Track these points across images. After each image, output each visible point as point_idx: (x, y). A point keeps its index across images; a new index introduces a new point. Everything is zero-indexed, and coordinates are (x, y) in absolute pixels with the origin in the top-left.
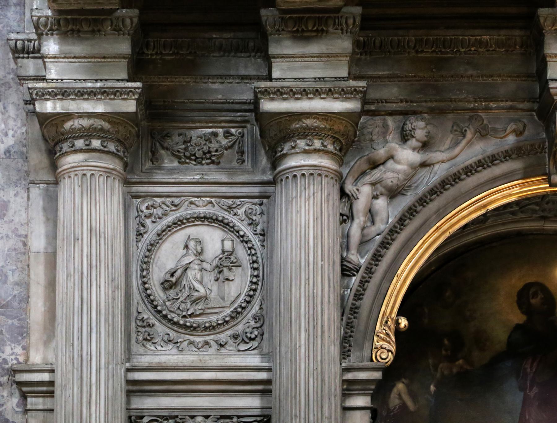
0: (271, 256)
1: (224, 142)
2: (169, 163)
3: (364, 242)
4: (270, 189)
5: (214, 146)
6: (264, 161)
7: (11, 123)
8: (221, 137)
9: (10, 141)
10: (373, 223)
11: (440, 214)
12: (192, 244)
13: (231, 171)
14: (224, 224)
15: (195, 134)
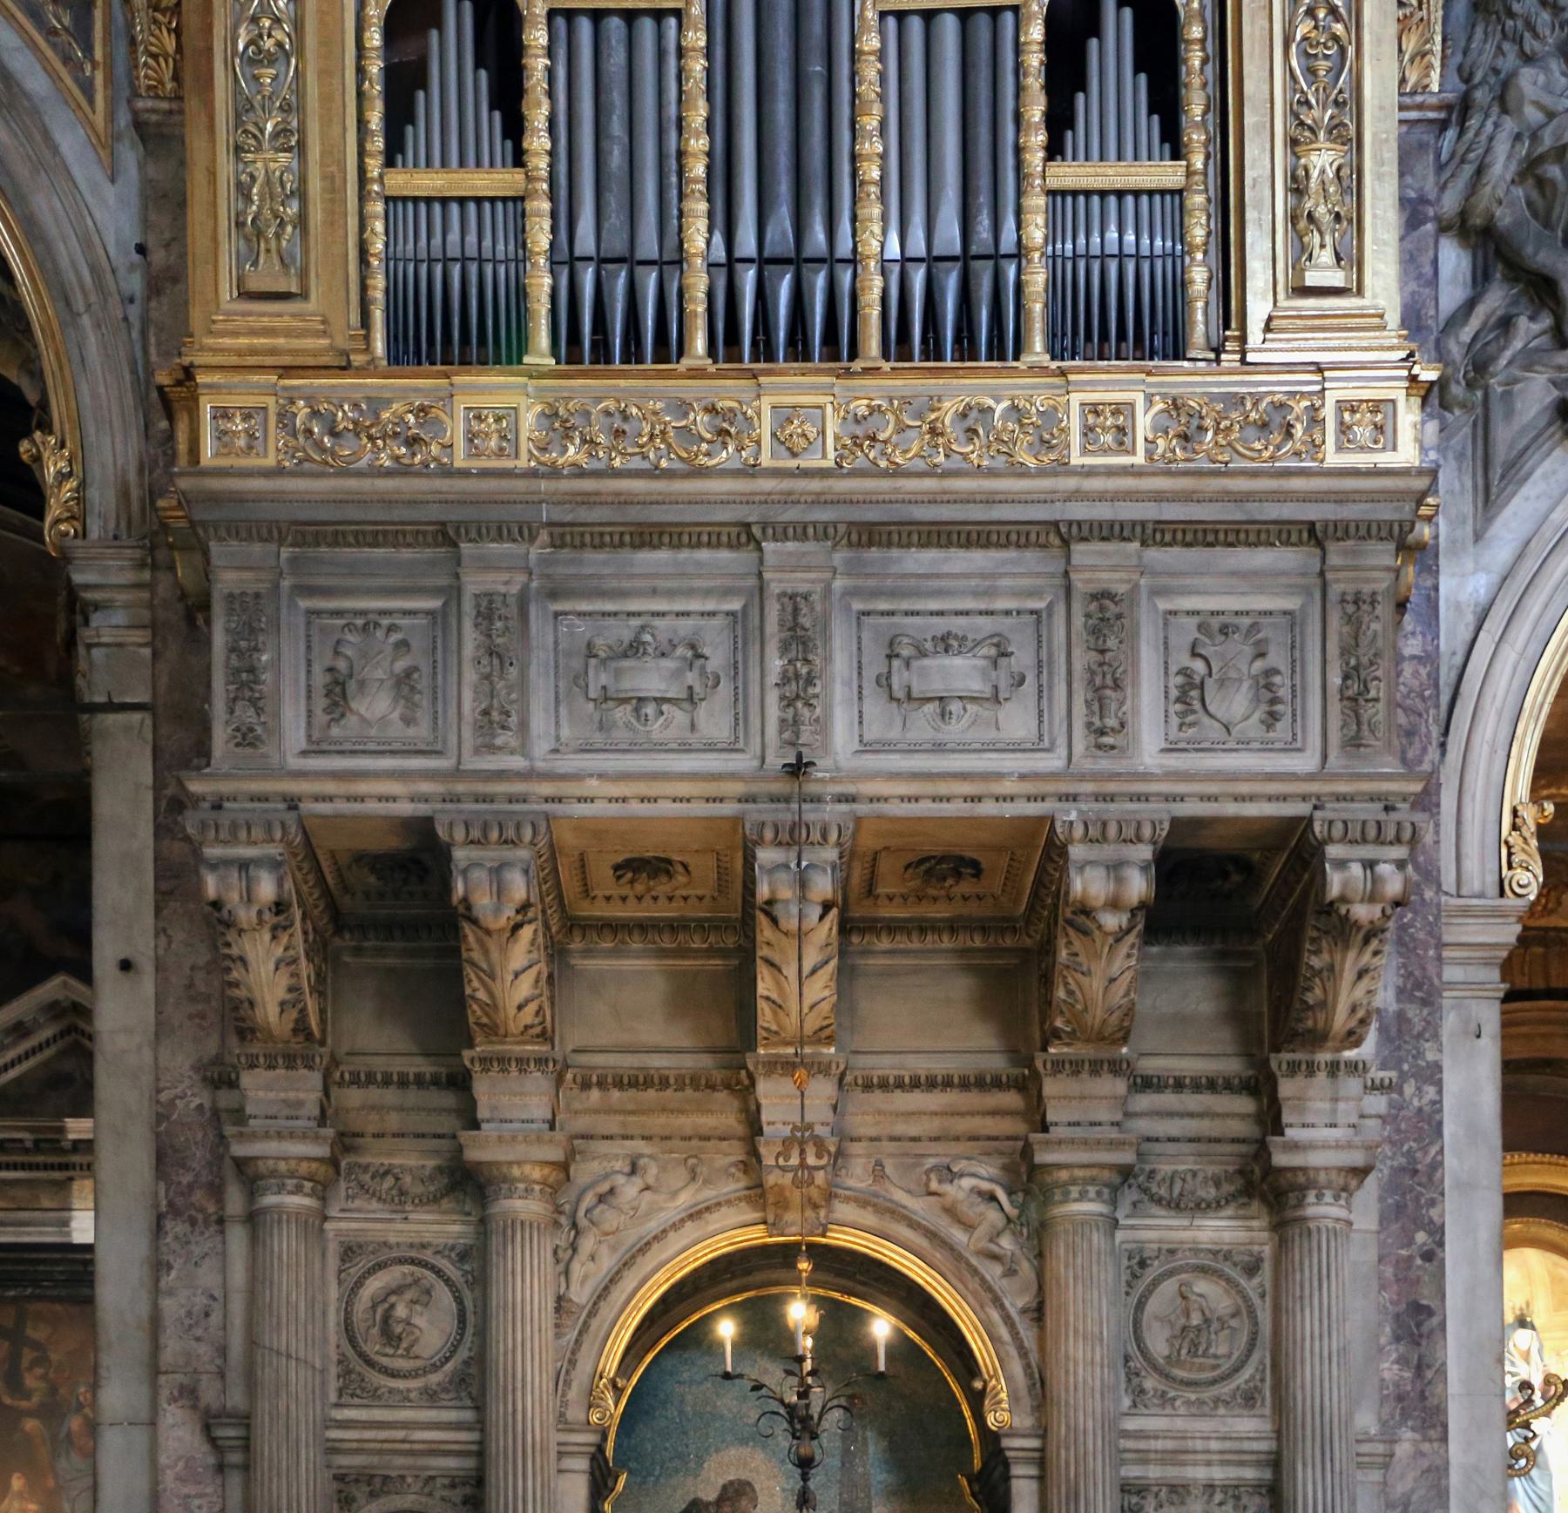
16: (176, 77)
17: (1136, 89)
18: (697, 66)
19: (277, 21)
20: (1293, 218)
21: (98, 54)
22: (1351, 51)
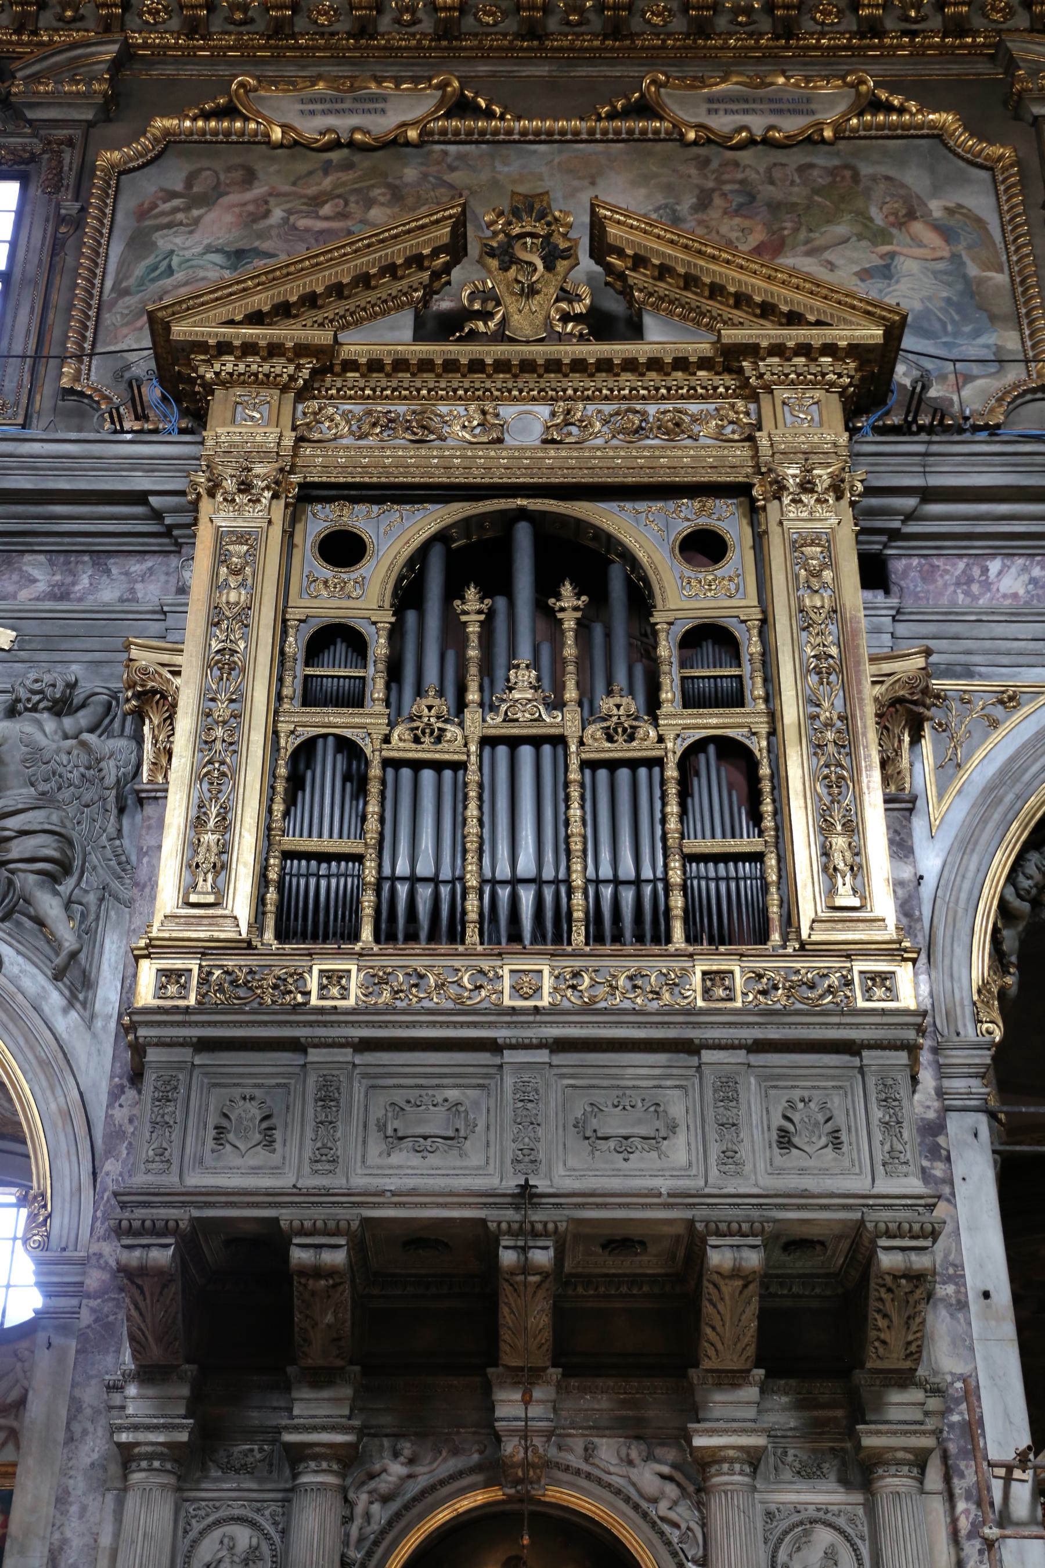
0: (286, 1552)
1: (258, 1456)
2: (215, 1473)
3: (361, 1540)
4: (290, 1495)
5: (250, 1459)
6: (287, 1472)
7: (98, 1441)
8: (256, 1453)
9: (95, 1456)
10: (369, 1523)
11: (421, 1517)
12: (226, 1540)
13: (261, 1480)
14: (253, 1524)
15: (236, 1450)
20: (825, 869)
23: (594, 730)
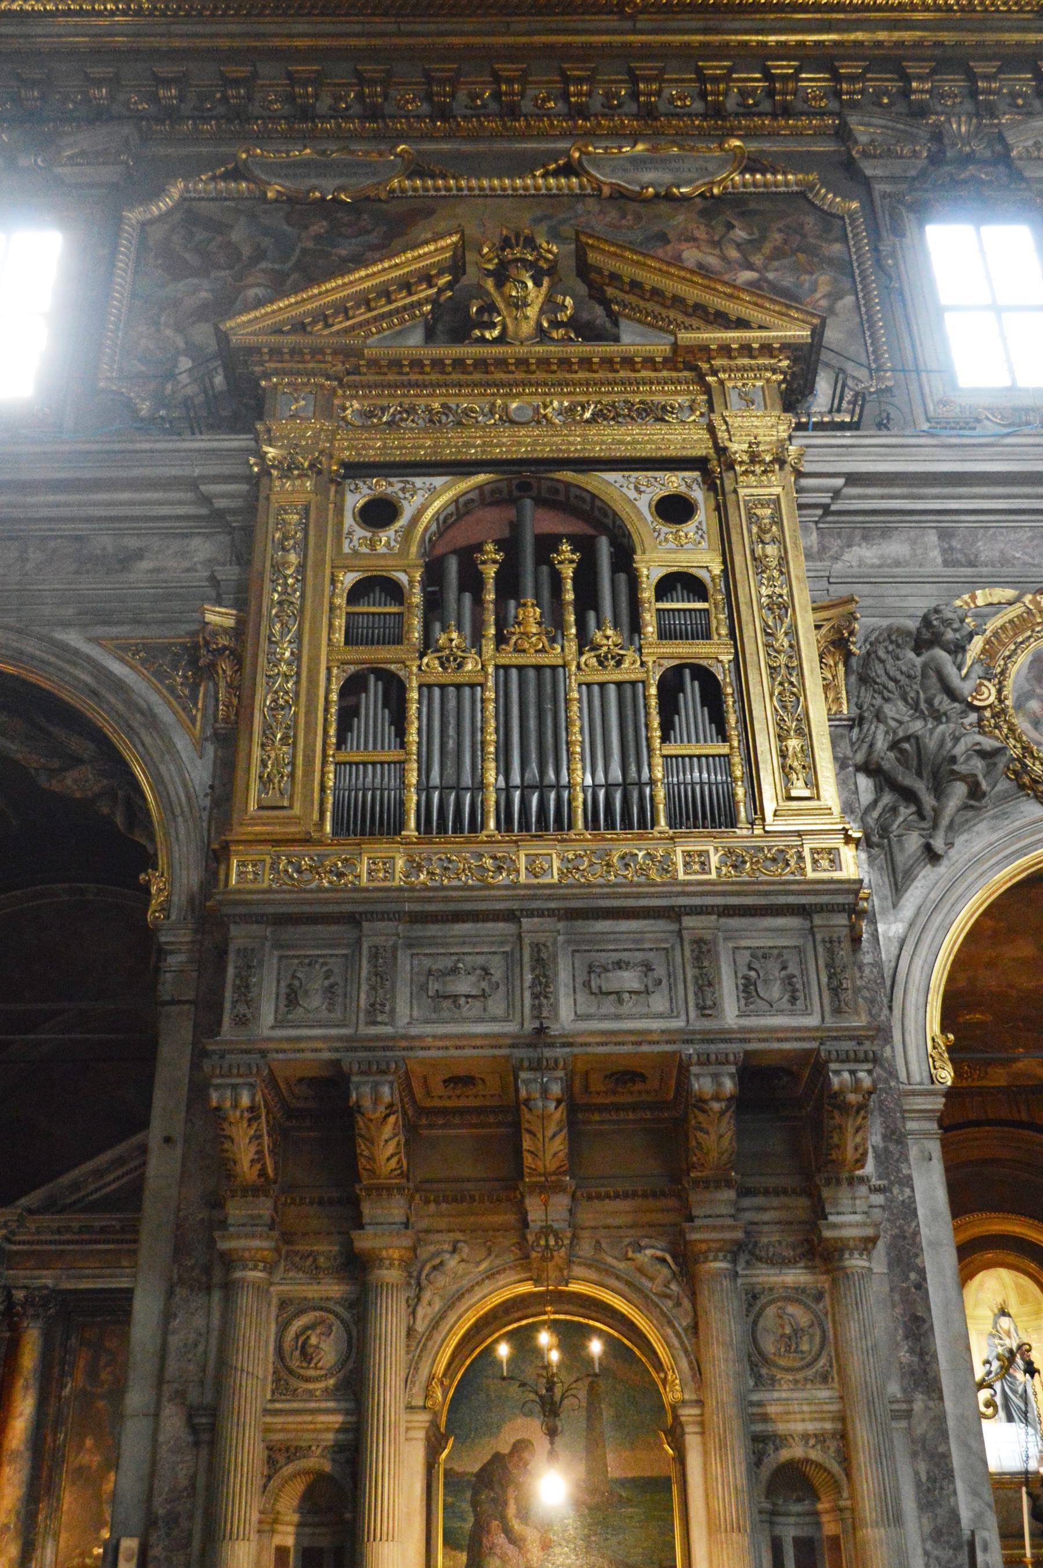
16: (237, 715)
17: (703, 714)
18: (491, 707)
19: (287, 693)
20: (783, 767)
21: (200, 705)
22: (802, 699)
23: (589, 658)
